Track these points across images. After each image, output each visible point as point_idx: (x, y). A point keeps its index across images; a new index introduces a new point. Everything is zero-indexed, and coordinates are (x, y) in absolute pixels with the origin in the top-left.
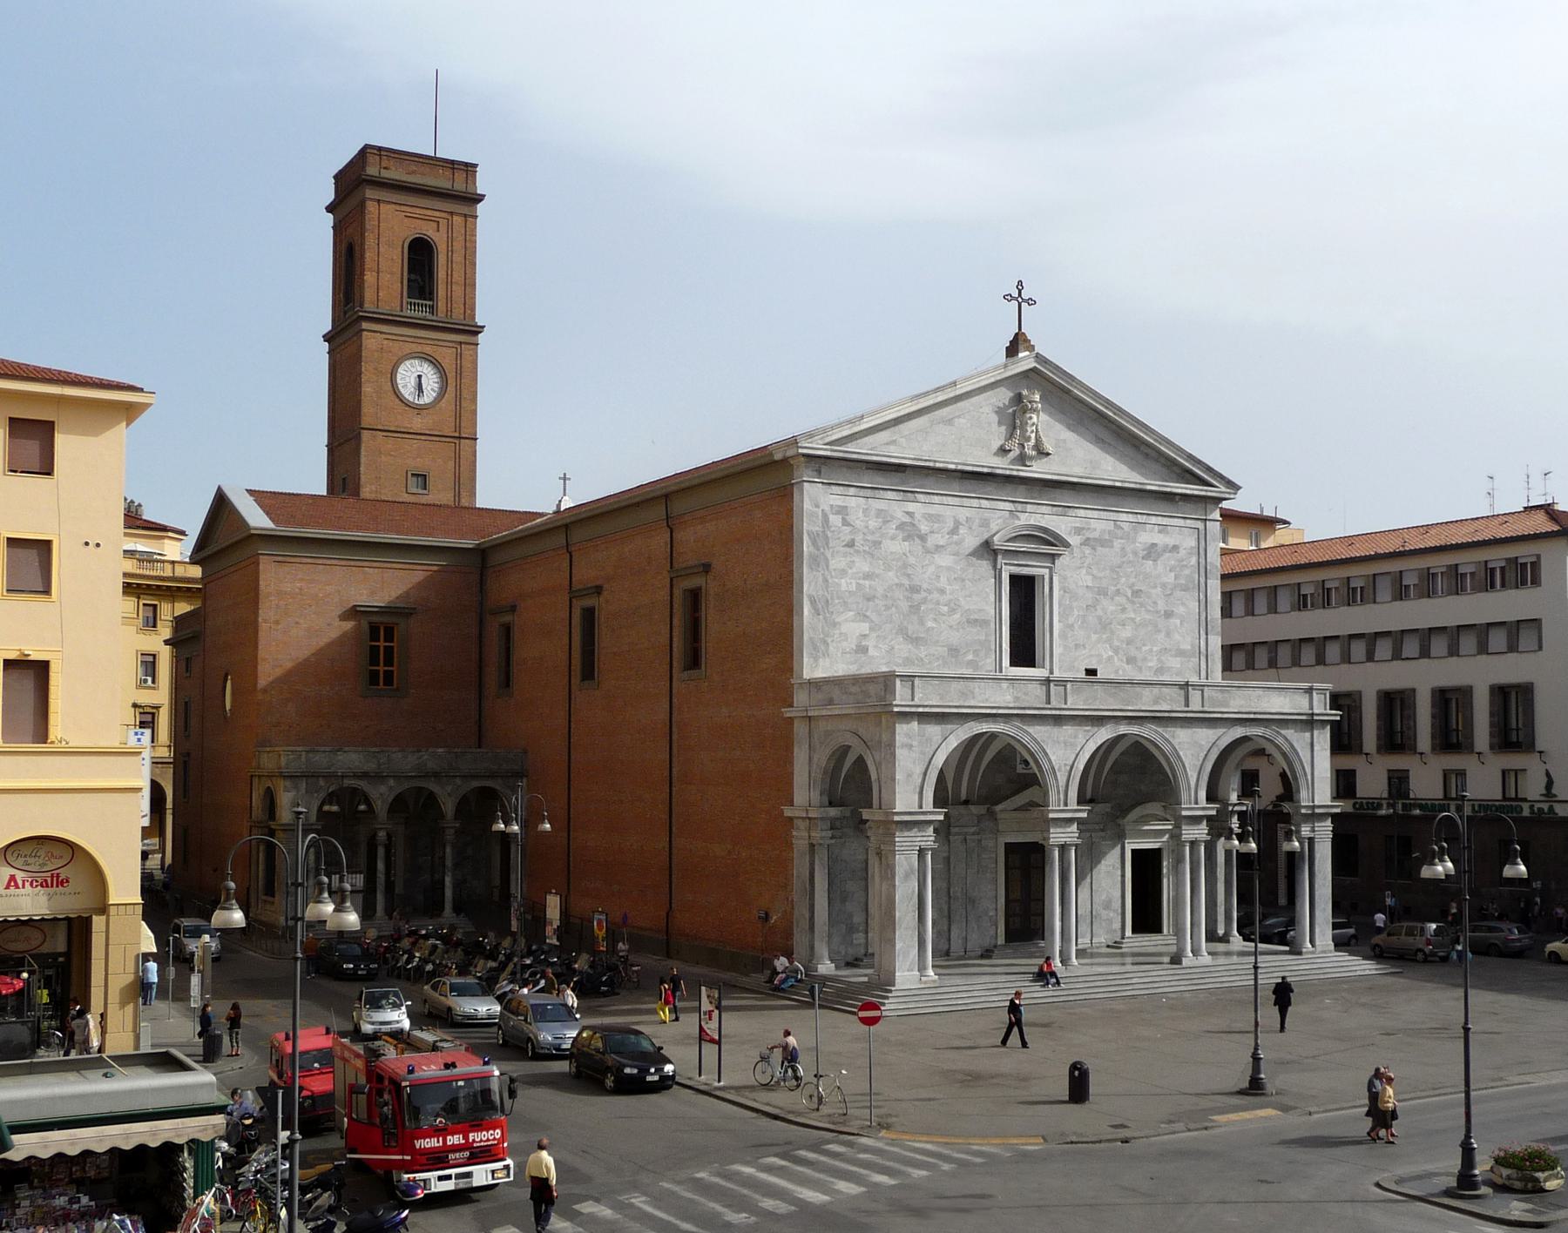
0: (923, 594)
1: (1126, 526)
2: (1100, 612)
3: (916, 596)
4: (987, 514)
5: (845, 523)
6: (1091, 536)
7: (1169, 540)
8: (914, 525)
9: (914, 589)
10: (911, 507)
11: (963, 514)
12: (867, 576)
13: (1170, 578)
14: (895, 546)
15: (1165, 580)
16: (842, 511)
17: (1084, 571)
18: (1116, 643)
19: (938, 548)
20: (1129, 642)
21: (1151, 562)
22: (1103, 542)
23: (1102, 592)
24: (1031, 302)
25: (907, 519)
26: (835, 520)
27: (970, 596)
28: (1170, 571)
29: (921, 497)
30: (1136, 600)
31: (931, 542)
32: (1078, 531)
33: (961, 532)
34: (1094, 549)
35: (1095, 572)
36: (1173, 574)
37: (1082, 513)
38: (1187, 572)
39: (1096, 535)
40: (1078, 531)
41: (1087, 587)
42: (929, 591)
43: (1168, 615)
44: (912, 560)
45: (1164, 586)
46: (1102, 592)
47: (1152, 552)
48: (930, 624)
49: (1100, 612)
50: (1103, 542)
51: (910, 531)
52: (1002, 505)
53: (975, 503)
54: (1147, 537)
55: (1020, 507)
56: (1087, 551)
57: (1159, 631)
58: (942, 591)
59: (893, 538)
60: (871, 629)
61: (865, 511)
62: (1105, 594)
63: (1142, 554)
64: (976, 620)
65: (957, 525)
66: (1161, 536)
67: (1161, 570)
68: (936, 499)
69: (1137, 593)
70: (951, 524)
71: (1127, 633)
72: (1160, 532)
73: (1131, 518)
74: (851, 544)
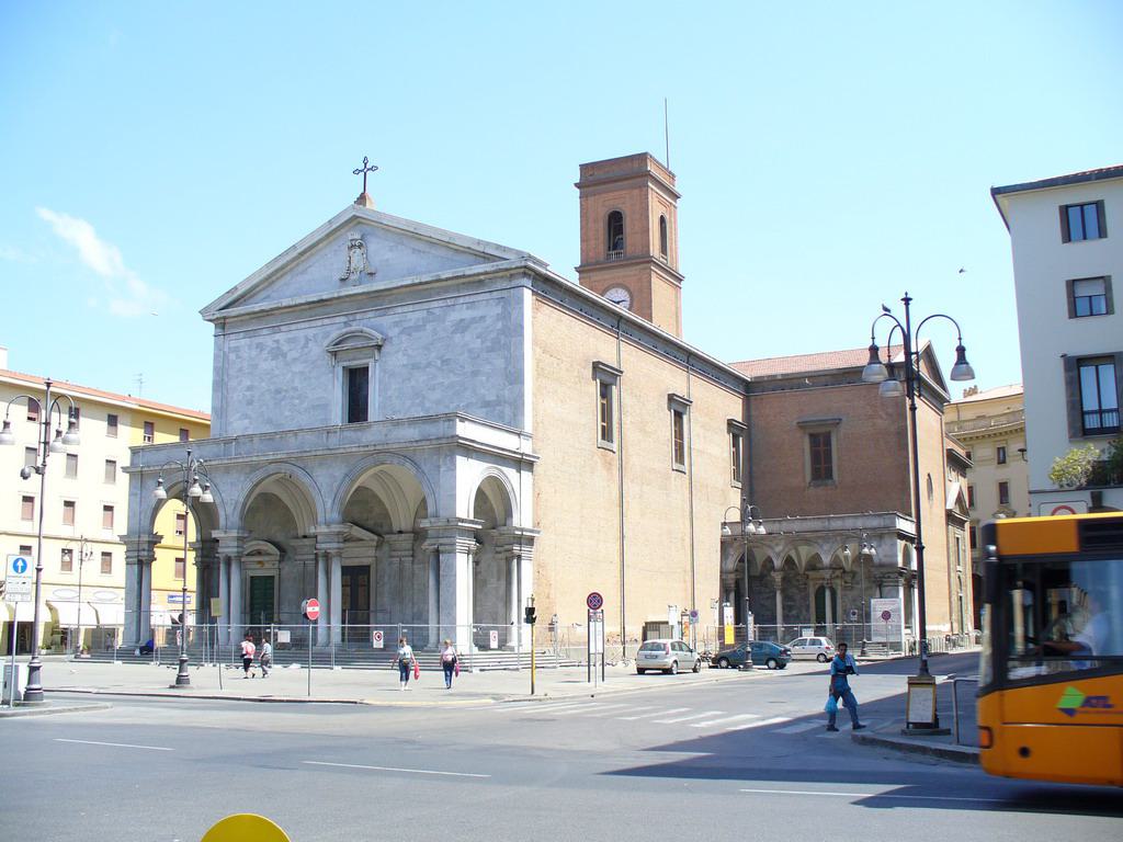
0: (283, 394)
1: (437, 311)
2: (413, 383)
3: (279, 396)
4: (328, 328)
5: (238, 357)
6: (406, 325)
8: (278, 348)
9: (278, 392)
10: (277, 336)
11: (311, 332)
12: (249, 388)
13: (477, 344)
14: (266, 365)
15: (472, 346)
16: (237, 350)
17: (401, 353)
18: (427, 405)
19: (295, 360)
20: (438, 402)
21: (459, 335)
23: (415, 367)
24: (374, 169)
25: (275, 345)
26: (232, 356)
27: (314, 389)
28: (478, 338)
29: (283, 328)
30: (445, 367)
31: (289, 357)
32: (396, 324)
33: (310, 345)
34: (409, 335)
35: (410, 352)
36: (479, 340)
37: (399, 310)
38: (493, 335)
39: (411, 324)
40: (396, 324)
41: (404, 365)
42: (286, 391)
43: (475, 374)
44: (277, 372)
45: (470, 351)
46: (415, 367)
47: (461, 326)
48: (287, 413)
49: (413, 383)
50: (417, 328)
51: (277, 353)
52: (337, 320)
53: (319, 323)
54: (455, 316)
55: (351, 318)
56: (404, 337)
57: (466, 389)
58: (295, 389)
59: (266, 360)
60: (251, 423)
61: (250, 347)
62: (419, 368)
63: (452, 330)
64: (318, 406)
65: (307, 340)
66: (469, 311)
67: (470, 339)
68: (293, 327)
69: (445, 362)
70: (303, 342)
71: (436, 395)
72: (468, 308)
73: (441, 303)
74: (240, 370)
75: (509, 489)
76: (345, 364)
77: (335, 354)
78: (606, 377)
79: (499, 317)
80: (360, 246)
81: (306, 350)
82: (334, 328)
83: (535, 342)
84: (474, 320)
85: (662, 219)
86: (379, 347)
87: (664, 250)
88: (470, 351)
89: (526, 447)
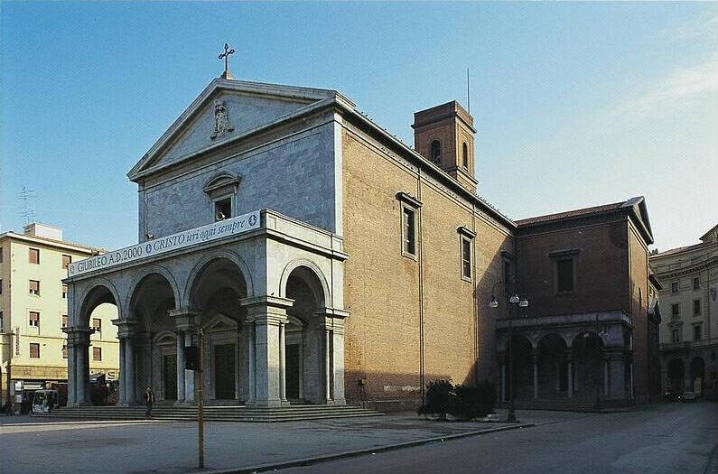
7: (301, 148)
22: (263, 166)
23: (261, 195)
26: (150, 205)
35: (257, 185)
43: (300, 195)
45: (297, 179)
47: (291, 160)
50: (263, 166)
51: (176, 199)
54: (287, 153)
55: (219, 165)
56: (253, 175)
68: (184, 178)
75: (322, 278)
76: (216, 200)
77: (209, 193)
78: (409, 205)
79: (317, 149)
80: (223, 110)
81: (192, 194)
82: (206, 173)
83: (346, 168)
84: (299, 154)
85: (465, 145)
86: (237, 184)
87: (465, 164)
88: (297, 179)
89: (337, 247)
